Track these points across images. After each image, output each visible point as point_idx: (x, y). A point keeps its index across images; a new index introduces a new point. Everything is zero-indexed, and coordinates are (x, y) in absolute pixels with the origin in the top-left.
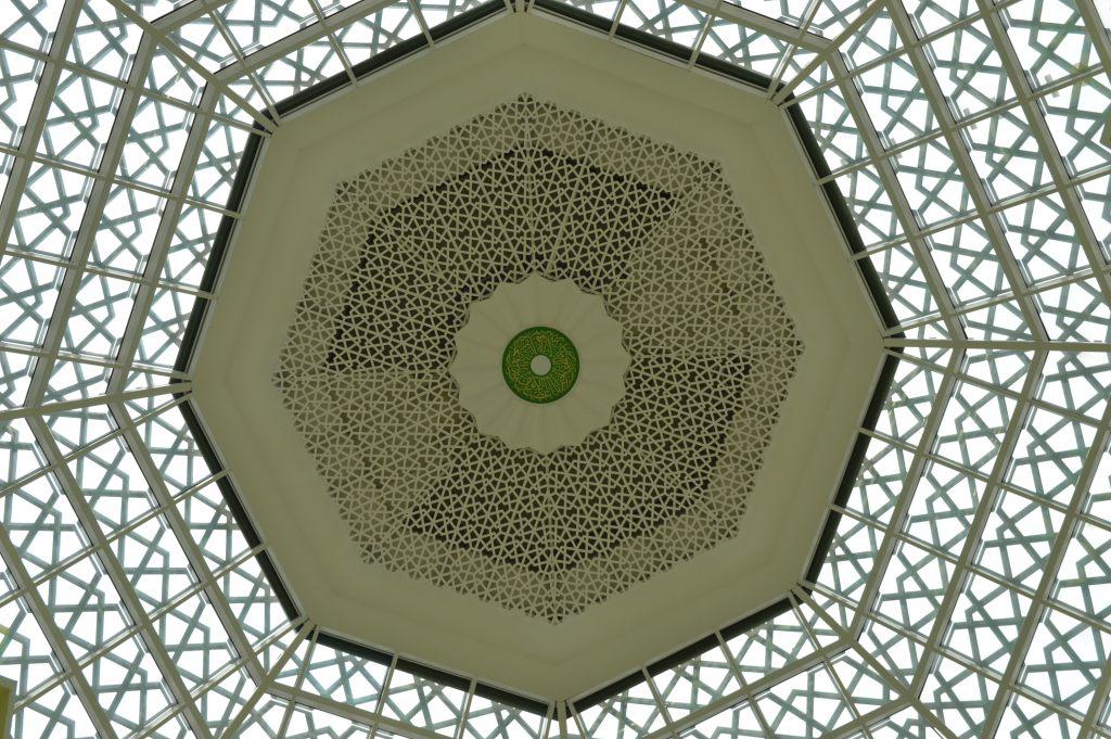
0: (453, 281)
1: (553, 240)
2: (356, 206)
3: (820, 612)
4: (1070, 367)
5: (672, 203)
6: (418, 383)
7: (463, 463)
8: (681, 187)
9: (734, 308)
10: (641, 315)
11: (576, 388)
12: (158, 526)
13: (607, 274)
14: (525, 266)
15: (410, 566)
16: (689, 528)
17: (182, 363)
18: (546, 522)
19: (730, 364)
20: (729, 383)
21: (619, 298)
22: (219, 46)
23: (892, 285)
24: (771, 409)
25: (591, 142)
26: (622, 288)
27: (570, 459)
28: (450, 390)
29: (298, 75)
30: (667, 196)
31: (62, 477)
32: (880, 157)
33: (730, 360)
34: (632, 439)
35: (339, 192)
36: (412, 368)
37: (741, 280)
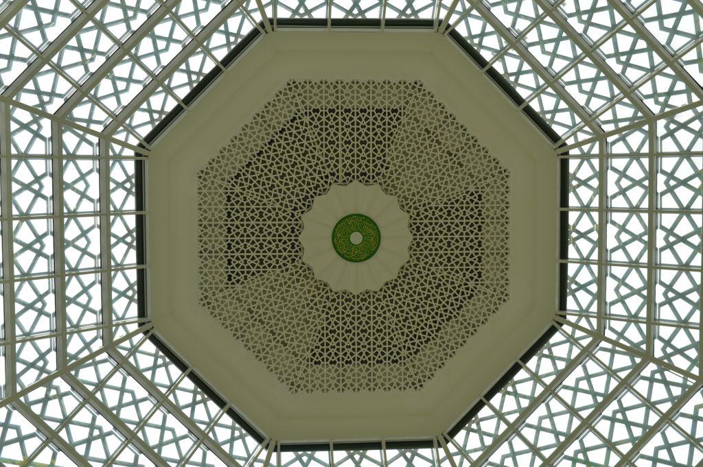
0: (286, 206)
1: (337, 161)
2: (213, 182)
3: (576, 326)
4: (672, 126)
5: (400, 114)
6: (287, 275)
7: (331, 313)
8: (402, 103)
10: (405, 187)
11: (383, 243)
13: (376, 170)
14: (326, 182)
15: (321, 386)
17: (142, 312)
18: (393, 331)
19: (468, 198)
20: (472, 210)
21: (389, 181)
23: (548, 116)
24: (503, 216)
25: (340, 95)
26: (388, 175)
27: (393, 288)
28: (307, 272)
29: (151, 116)
30: (395, 111)
31: (95, 404)
32: (515, 42)
33: (468, 195)
34: (426, 263)
35: (200, 177)
36: (280, 267)
37: (457, 145)
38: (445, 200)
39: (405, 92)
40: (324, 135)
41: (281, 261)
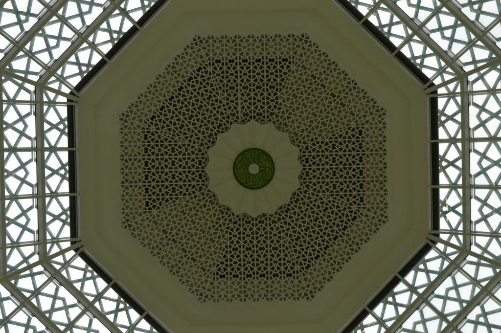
6: (195, 201)
9: (342, 104)
10: (296, 125)
11: (277, 173)
12: (88, 319)
15: (226, 296)
16: (361, 225)
19: (350, 133)
20: (354, 143)
22: (35, 67)
24: (381, 149)
27: (287, 211)
28: (213, 198)
30: (286, 60)
34: (315, 190)
35: (122, 119)
37: (340, 88)
38: (330, 135)
39: (293, 44)
40: (225, 81)
41: (191, 190)
